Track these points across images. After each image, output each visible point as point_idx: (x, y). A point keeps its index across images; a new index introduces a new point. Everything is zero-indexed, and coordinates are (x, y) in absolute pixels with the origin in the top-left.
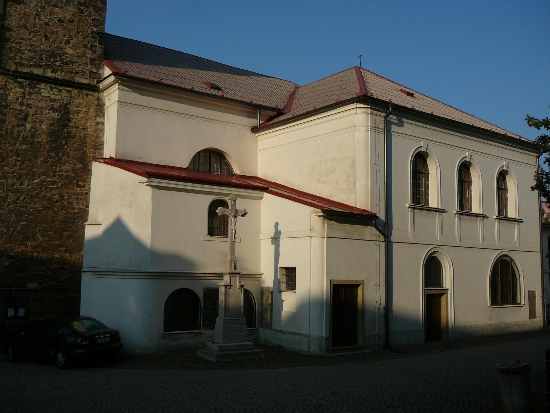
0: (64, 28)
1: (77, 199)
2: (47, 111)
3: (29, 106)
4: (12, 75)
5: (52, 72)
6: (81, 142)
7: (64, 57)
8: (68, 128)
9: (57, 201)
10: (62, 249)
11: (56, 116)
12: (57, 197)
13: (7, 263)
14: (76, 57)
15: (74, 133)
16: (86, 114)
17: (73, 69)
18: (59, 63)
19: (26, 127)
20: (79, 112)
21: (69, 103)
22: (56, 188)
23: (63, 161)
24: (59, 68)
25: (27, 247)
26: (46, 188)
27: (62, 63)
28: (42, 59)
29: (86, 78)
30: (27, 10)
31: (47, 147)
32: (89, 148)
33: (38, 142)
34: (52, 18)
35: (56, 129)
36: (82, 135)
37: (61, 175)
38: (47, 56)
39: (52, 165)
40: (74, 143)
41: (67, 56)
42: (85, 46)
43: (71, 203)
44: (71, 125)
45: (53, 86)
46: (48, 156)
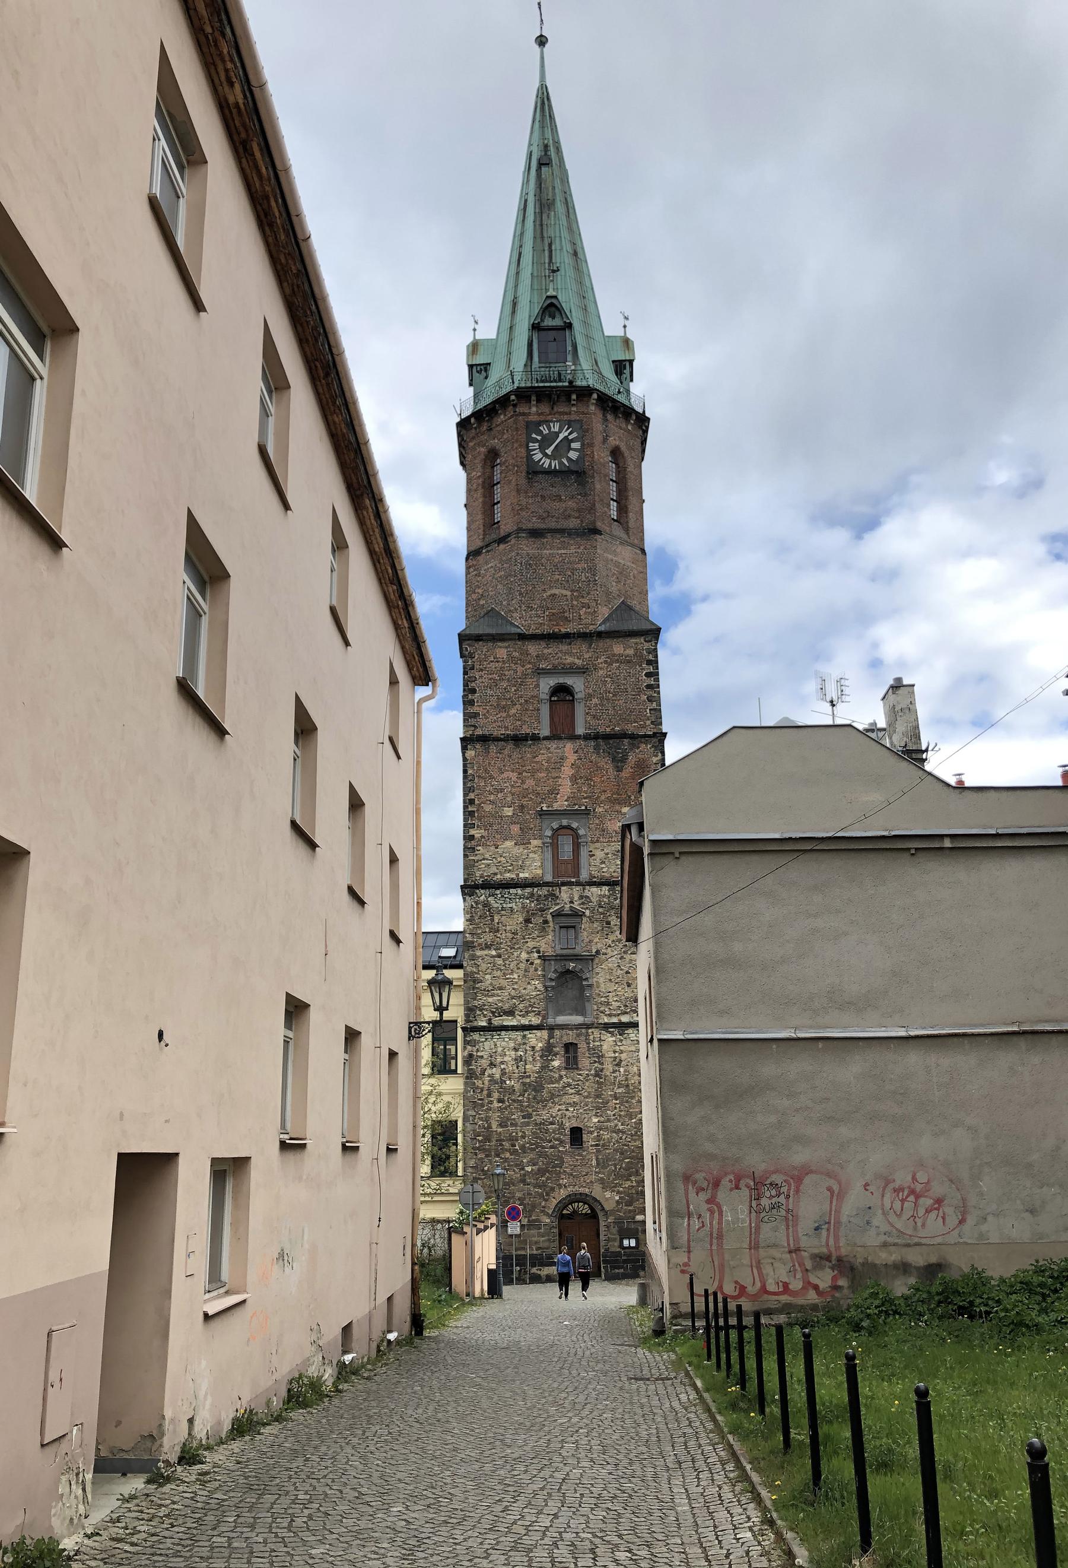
3: (622, 1052)
4: (604, 1027)
13: (617, 1198)
34: (631, 965)
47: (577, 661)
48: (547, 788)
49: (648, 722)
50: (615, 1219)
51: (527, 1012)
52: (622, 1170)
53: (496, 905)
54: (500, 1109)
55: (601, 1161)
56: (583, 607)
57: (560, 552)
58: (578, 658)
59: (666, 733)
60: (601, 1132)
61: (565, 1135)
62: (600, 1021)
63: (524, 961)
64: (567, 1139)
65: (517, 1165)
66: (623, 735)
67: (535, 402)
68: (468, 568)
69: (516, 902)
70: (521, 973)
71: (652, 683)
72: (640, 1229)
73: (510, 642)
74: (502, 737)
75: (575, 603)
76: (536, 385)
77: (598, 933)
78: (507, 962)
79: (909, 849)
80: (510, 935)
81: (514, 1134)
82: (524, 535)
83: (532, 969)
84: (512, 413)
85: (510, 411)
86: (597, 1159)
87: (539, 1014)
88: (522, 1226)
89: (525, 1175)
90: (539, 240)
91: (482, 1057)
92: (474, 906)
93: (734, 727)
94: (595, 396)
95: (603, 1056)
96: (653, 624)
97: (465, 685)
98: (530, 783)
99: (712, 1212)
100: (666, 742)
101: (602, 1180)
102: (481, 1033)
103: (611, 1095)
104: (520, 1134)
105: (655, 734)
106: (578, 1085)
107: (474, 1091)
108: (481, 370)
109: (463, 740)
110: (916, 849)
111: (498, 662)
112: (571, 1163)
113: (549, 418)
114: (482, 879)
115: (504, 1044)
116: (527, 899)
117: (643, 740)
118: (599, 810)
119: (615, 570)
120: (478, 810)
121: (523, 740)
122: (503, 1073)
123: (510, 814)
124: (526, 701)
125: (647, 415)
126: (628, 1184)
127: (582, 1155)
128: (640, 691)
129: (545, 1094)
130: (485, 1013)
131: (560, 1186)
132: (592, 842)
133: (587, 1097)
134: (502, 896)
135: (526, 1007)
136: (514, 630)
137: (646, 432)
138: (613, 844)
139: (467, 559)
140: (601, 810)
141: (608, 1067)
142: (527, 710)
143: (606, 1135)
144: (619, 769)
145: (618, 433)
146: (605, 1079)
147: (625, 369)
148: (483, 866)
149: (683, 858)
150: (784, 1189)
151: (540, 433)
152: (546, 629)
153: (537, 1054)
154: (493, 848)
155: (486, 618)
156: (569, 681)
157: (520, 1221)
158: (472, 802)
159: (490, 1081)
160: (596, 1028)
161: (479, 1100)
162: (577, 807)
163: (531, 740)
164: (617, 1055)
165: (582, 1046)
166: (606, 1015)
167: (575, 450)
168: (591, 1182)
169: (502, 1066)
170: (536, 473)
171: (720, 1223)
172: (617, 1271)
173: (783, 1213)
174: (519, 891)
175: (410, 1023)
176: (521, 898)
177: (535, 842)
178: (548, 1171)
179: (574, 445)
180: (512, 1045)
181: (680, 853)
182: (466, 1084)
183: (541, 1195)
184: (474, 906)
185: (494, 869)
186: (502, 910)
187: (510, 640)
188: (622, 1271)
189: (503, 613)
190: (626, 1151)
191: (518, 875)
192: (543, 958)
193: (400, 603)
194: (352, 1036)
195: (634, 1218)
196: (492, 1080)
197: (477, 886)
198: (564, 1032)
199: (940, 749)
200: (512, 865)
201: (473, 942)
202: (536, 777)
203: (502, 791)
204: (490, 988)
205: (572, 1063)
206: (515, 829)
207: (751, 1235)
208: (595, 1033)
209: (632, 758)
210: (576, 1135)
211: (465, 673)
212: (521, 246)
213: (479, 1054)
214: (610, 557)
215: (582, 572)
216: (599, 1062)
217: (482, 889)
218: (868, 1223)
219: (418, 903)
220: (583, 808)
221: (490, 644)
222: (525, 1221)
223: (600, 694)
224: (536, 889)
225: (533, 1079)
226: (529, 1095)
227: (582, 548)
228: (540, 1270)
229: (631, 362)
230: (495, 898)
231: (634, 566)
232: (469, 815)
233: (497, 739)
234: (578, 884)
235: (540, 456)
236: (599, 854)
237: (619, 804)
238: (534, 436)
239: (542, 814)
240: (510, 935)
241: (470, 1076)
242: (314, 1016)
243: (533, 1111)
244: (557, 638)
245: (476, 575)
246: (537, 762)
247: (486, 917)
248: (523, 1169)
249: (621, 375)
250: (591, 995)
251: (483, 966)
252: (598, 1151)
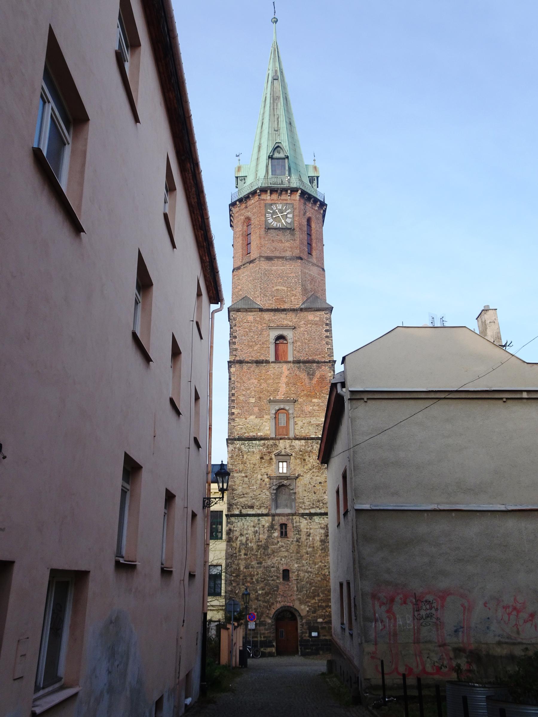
0: (322, 486)
2: (319, 530)
3: (311, 529)
4: (301, 516)
9: (328, 575)
11: (323, 531)
13: (308, 609)
19: (309, 539)
24: (322, 507)
25: (316, 600)
26: (322, 569)
27: (323, 504)
28: (314, 504)
30: (305, 482)
31: (321, 548)
33: (316, 546)
34: (316, 482)
35: (324, 538)
39: (323, 557)
41: (325, 500)
45: (320, 516)
46: (322, 552)
47: (289, 323)
48: (274, 388)
49: (326, 355)
50: (306, 621)
51: (261, 507)
52: (311, 594)
53: (245, 450)
54: (245, 559)
55: (299, 588)
56: (293, 296)
57: (281, 268)
58: (290, 322)
59: (336, 361)
60: (300, 572)
61: (280, 574)
62: (299, 512)
63: (260, 480)
64: (281, 576)
65: (254, 590)
66: (313, 362)
67: (269, 194)
68: (233, 276)
69: (256, 448)
70: (258, 486)
71: (329, 335)
72: (320, 627)
73: (255, 313)
74: (250, 361)
75: (289, 293)
76: (270, 186)
77: (299, 465)
78: (250, 480)
79: (502, 399)
80: (252, 466)
81: (252, 573)
82: (263, 259)
83: (264, 484)
84: (258, 199)
85: (257, 197)
86: (297, 587)
87: (267, 508)
88: (256, 624)
89: (258, 596)
90: (272, 116)
91: (236, 531)
92: (234, 450)
93: (398, 327)
94: (300, 191)
95: (301, 531)
96: (329, 305)
97: (231, 334)
98: (264, 386)
99: (390, 619)
100: (335, 365)
101: (299, 599)
102: (236, 518)
103: (305, 552)
104: (256, 573)
105: (330, 362)
106: (287, 546)
107: (231, 549)
108: (242, 179)
109: (229, 362)
110: (507, 399)
111: (248, 322)
112: (283, 589)
113: (277, 202)
114: (238, 436)
115: (248, 524)
116: (262, 446)
117: (323, 364)
118: (300, 400)
119: (309, 278)
120: (236, 399)
121: (261, 363)
122: (247, 539)
123: (253, 401)
124: (263, 343)
125: (326, 202)
126: (313, 601)
127: (289, 585)
128: (322, 339)
129: (270, 551)
130: (238, 507)
131: (277, 602)
132: (297, 417)
133: (292, 553)
134: (248, 445)
135: (260, 504)
136: (256, 306)
137: (325, 211)
138: (307, 418)
139: (233, 271)
140: (301, 400)
141: (304, 537)
142: (263, 347)
143: (302, 574)
144: (311, 379)
145: (311, 210)
146: (302, 544)
147: (314, 180)
148: (239, 429)
149: (369, 401)
150: (435, 605)
151: (272, 209)
152: (274, 307)
153: (265, 530)
154: (244, 419)
155: (242, 300)
156: (285, 333)
157: (255, 621)
158: (233, 395)
159: (240, 543)
160: (297, 515)
161: (234, 554)
162: (288, 399)
163: (265, 363)
164: (308, 530)
165: (290, 526)
166: (303, 509)
167: (289, 218)
168: (294, 600)
169: (247, 536)
170: (269, 229)
171: (395, 625)
172: (307, 651)
173: (434, 620)
174: (257, 442)
175: (204, 498)
176: (258, 446)
177: (266, 417)
178: (271, 594)
179: (288, 216)
180: (252, 524)
181: (368, 399)
182: (227, 545)
183: (267, 607)
184: (234, 450)
185: (244, 431)
186: (248, 452)
187: (255, 311)
188: (310, 650)
189: (251, 298)
190: (313, 583)
191: (257, 434)
192: (270, 478)
193: (205, 244)
194: (170, 497)
195: (317, 620)
196: (242, 544)
197: (235, 439)
198: (280, 517)
199: (513, 345)
200: (254, 428)
201: (232, 469)
202: (267, 382)
203: (249, 389)
204: (241, 494)
205: (284, 534)
206: (256, 409)
207: (415, 634)
208: (297, 518)
209: (318, 374)
210: (286, 574)
211: (231, 328)
212: (263, 119)
213: (235, 529)
214: (307, 271)
215: (292, 278)
216: (299, 534)
217: (238, 440)
218: (488, 628)
219: (209, 428)
220: (292, 399)
221: (244, 313)
222: (258, 622)
223: (302, 340)
224: (266, 441)
225: (263, 543)
226: (261, 551)
227: (292, 266)
228: (265, 649)
229: (318, 177)
230: (245, 446)
231: (319, 277)
232: (232, 401)
233: (248, 362)
234: (289, 439)
235: (272, 220)
236: (300, 424)
237: (311, 397)
238: (269, 210)
239: (270, 401)
240: (252, 466)
241: (230, 540)
242: (145, 475)
243: (263, 560)
244: (279, 311)
245: (238, 279)
246: (268, 375)
247: (239, 456)
248: (257, 592)
249: (312, 183)
250: (295, 498)
251: (238, 482)
252: (298, 583)
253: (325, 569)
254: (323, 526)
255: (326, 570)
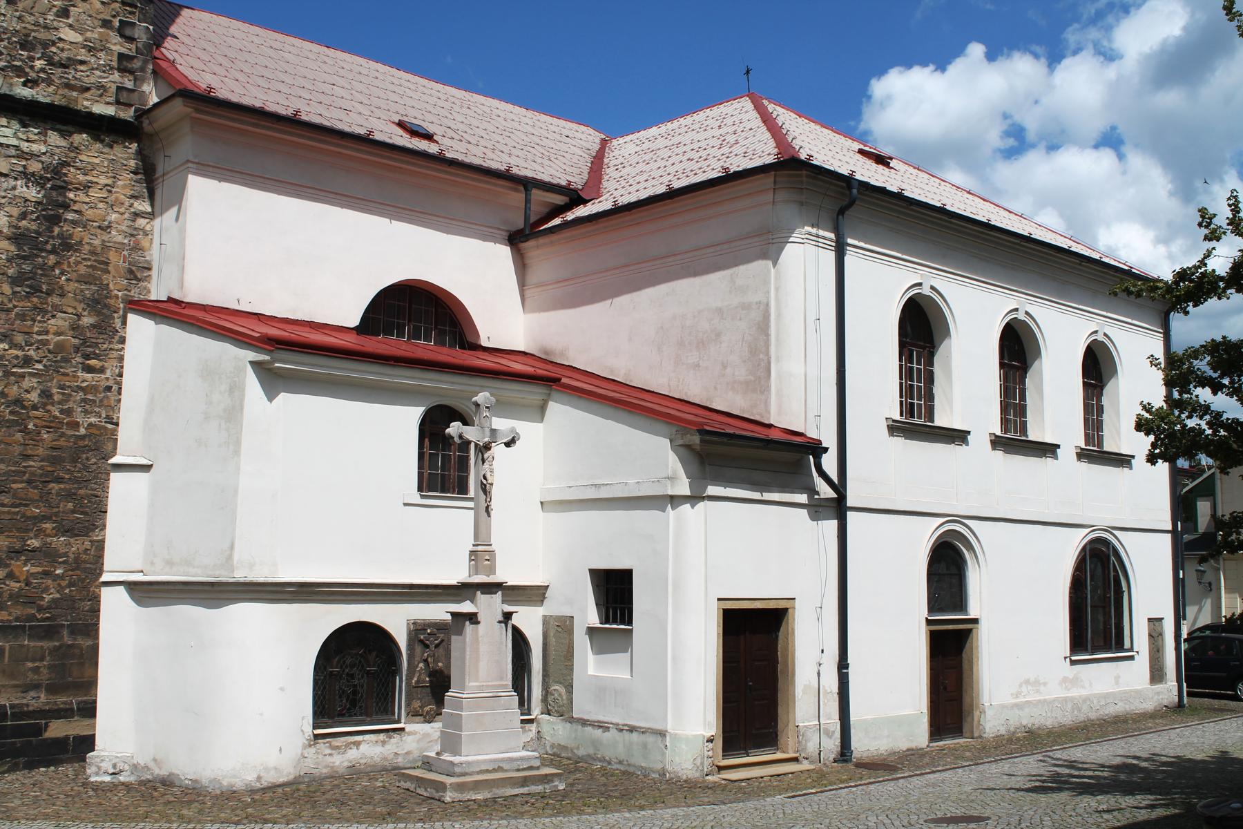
1: (84, 400)
5: (25, 84)
6: (95, 261)
7: (54, 49)
8: (61, 224)
9: (35, 407)
10: (48, 526)
11: (33, 193)
12: (34, 397)
14: (83, 50)
15: (76, 239)
16: (110, 191)
17: (76, 78)
18: (39, 64)
20: (89, 187)
21: (65, 164)
22: (31, 374)
23: (50, 308)
24: (42, 75)
27: (51, 62)
29: (108, 103)
32: (114, 277)
35: (34, 226)
36: (96, 242)
37: (45, 343)
38: (11, 44)
39: (22, 317)
40: (77, 263)
41: (61, 45)
42: (106, 24)
43: (69, 412)
44: (70, 216)
46: (14, 293)
253: (22, 376)
254: (35, 167)
255: (27, 383)
